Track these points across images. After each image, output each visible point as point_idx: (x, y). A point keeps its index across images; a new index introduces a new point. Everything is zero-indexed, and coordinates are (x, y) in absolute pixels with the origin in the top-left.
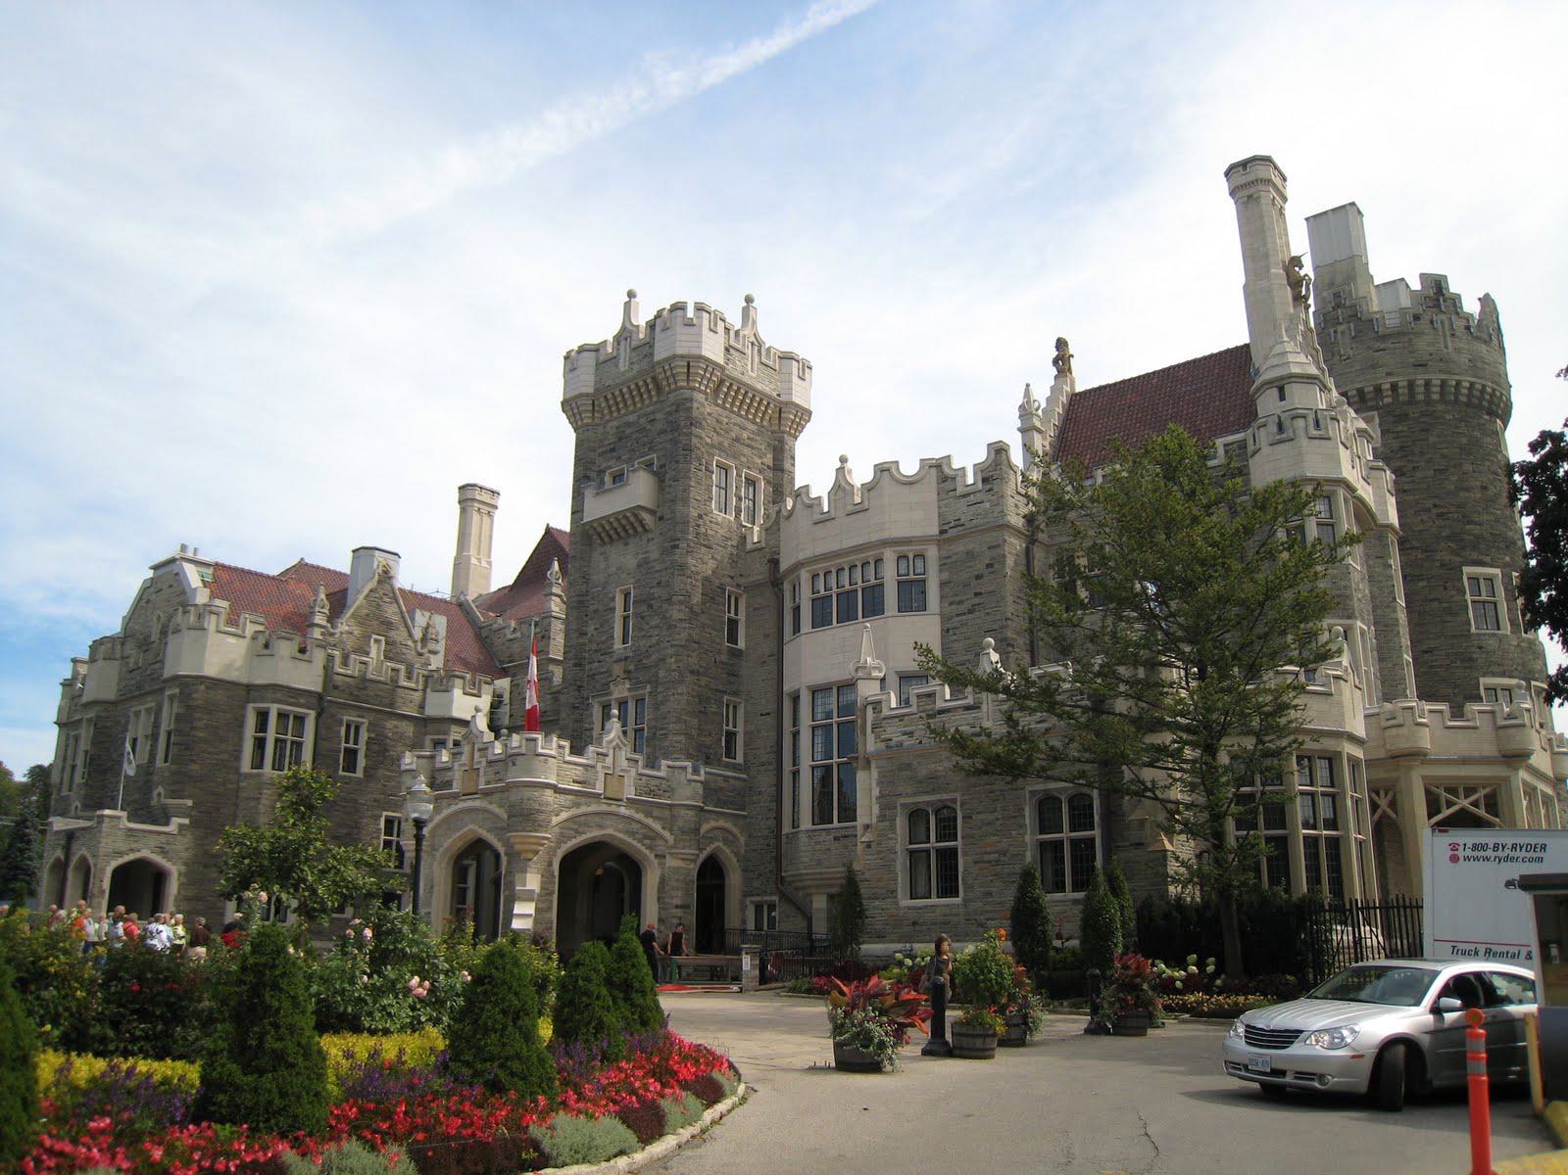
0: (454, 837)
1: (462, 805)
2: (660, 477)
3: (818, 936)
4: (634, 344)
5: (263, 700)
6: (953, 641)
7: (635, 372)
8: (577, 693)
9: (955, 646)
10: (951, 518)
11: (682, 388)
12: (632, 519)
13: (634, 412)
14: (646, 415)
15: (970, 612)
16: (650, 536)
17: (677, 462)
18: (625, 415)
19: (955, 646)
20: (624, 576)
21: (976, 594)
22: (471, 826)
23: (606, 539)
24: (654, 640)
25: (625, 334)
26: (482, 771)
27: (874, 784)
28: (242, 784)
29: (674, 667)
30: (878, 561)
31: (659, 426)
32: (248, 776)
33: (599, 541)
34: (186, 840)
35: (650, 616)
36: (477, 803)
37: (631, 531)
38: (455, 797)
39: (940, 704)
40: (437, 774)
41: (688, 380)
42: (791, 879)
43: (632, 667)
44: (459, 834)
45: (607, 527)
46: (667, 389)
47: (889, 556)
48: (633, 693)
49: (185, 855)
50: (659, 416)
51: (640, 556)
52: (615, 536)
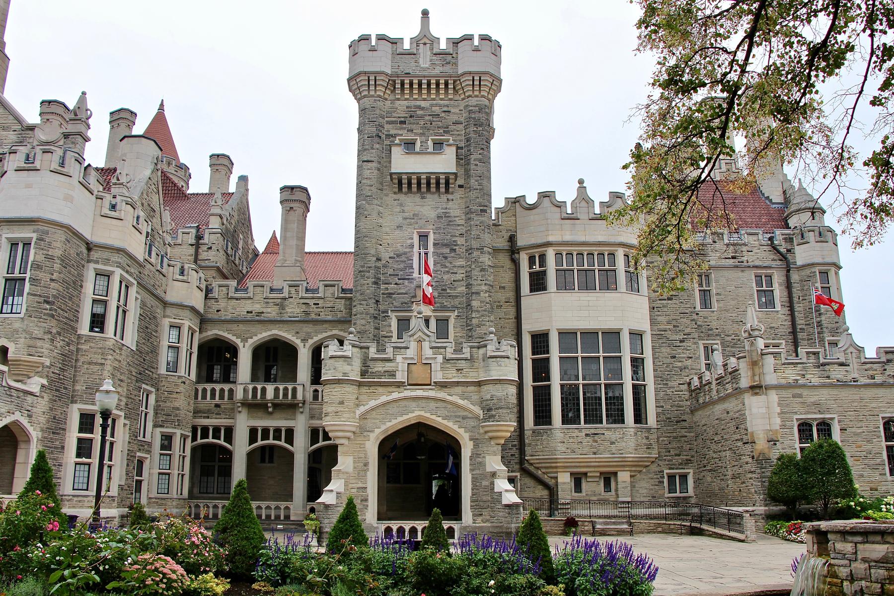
0: (394, 422)
2: (462, 159)
3: (563, 501)
5: (107, 261)
11: (483, 96)
12: (442, 181)
13: (424, 100)
14: (436, 105)
15: (669, 299)
16: (450, 197)
18: (416, 99)
20: (422, 222)
22: (417, 413)
23: (405, 189)
24: (459, 277)
25: (425, 39)
26: (436, 366)
27: (776, 405)
28: (84, 347)
29: (488, 300)
30: (612, 255)
31: (455, 118)
32: (89, 339)
33: (397, 190)
34: (44, 403)
35: (453, 257)
36: (431, 394)
37: (433, 190)
38: (399, 385)
39: (822, 360)
41: (488, 93)
42: (532, 462)
44: (400, 419)
45: (414, 181)
46: (471, 93)
47: (620, 253)
49: (42, 419)
50: (453, 110)
51: (440, 210)
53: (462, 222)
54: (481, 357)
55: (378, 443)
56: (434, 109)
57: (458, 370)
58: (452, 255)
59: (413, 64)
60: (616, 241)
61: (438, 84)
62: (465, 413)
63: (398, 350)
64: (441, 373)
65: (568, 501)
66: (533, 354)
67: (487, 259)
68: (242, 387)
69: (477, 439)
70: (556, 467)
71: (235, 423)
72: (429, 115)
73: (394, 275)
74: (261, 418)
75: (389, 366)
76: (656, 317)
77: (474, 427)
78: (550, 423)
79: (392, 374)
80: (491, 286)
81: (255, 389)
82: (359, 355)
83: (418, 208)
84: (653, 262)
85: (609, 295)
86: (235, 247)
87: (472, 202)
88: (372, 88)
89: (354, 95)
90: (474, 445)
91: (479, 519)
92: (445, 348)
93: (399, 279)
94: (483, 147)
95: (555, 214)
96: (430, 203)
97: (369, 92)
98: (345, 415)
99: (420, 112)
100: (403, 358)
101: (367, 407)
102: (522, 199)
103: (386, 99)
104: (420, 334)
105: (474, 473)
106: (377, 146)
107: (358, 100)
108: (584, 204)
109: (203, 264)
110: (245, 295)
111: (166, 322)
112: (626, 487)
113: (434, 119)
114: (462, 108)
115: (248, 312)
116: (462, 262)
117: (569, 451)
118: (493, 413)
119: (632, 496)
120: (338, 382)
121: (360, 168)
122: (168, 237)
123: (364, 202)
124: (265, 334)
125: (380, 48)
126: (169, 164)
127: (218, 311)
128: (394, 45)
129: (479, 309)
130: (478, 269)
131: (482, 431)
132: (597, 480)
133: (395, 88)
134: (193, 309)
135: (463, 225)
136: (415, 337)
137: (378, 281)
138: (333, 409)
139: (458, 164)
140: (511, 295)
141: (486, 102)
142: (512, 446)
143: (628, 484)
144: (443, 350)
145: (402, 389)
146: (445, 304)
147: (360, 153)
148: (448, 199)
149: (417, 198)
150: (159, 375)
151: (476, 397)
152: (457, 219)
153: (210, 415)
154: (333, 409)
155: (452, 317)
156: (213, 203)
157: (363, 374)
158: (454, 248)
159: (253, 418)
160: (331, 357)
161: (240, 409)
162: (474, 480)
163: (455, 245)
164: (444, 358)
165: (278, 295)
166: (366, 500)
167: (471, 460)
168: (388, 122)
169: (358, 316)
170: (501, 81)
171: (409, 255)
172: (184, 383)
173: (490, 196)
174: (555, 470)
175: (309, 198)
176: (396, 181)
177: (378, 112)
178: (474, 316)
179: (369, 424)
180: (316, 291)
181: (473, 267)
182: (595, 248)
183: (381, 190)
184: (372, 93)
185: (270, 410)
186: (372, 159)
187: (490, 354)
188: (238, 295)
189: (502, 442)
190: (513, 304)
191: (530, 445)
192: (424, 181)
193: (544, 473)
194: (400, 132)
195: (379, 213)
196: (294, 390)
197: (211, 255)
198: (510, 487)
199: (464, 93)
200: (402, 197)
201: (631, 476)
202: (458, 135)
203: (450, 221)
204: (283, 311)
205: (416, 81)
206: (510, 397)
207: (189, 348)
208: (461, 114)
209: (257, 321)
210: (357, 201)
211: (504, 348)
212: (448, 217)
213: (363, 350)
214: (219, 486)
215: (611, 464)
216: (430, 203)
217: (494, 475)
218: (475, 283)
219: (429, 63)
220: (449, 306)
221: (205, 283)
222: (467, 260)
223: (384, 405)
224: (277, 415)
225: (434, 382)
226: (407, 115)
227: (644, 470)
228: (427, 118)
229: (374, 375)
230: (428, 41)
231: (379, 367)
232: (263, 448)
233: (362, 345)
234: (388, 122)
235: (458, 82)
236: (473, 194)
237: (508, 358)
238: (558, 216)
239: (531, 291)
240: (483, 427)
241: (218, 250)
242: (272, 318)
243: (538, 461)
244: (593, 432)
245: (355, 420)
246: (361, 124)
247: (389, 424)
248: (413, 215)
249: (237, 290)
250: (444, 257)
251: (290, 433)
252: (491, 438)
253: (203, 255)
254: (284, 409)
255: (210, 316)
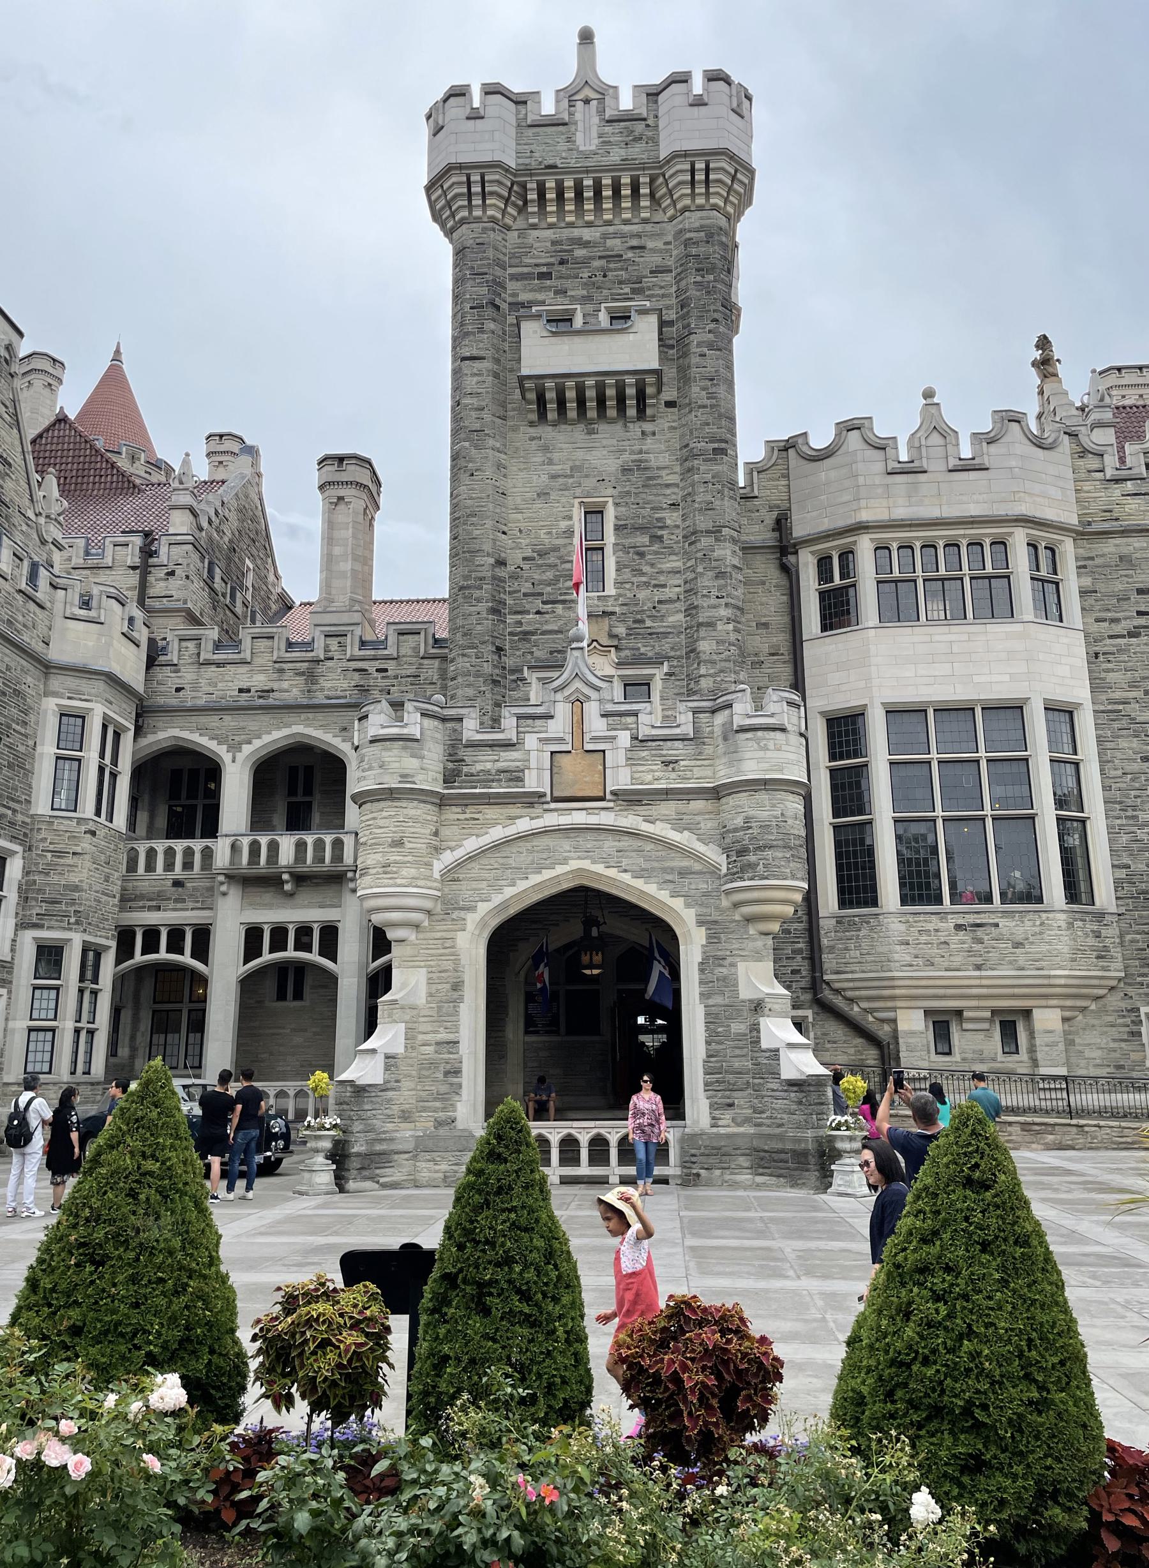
0: (522, 885)
1: (551, 820)
3: (913, 1073)
4: (608, 114)
6: (1108, 671)
7: (616, 155)
8: (496, 657)
9: (1111, 677)
10: (1094, 508)
11: (715, 208)
13: (589, 225)
14: (615, 235)
15: (1131, 635)
16: (648, 427)
17: (715, 320)
18: (571, 225)
19: (1111, 677)
20: (590, 483)
21: (1140, 613)
22: (574, 864)
23: (552, 415)
24: (670, 593)
26: (616, 757)
29: (733, 637)
30: (1000, 543)
31: (656, 260)
33: (534, 417)
35: (656, 553)
36: (607, 819)
37: (612, 413)
38: (533, 800)
40: (462, 753)
41: (726, 200)
42: (837, 985)
43: (621, 630)
44: (535, 879)
46: (687, 201)
47: (1019, 539)
48: (620, 672)
50: (650, 244)
51: (626, 457)
52: (572, 414)
53: (674, 479)
54: (718, 731)
55: (486, 934)
56: (609, 243)
57: (666, 764)
58: (655, 547)
59: (562, 146)
60: (1010, 513)
61: (616, 188)
62: (686, 863)
63: (530, 722)
64: (628, 770)
65: (924, 1073)
66: (833, 757)
67: (728, 552)
68: (228, 841)
69: (716, 922)
70: (893, 998)
71: (215, 917)
72: (600, 258)
73: (533, 595)
74: (269, 906)
75: (508, 759)
76: (1103, 675)
77: (706, 894)
78: (874, 902)
79: (516, 776)
80: (738, 608)
81: (255, 848)
82: (439, 736)
83: (580, 455)
84: (1092, 558)
85: (998, 630)
86: (237, 586)
87: (695, 434)
88: (477, 201)
89: (443, 226)
90: (709, 937)
91: (727, 1117)
92: (635, 714)
93: (544, 603)
94: (716, 315)
95: (875, 464)
96: (605, 442)
97: (470, 212)
98: (404, 872)
99: (580, 253)
100: (540, 740)
101: (460, 853)
102: (800, 441)
103: (509, 228)
104: (578, 684)
105: (711, 1002)
106: (491, 325)
107: (449, 233)
108: (936, 439)
109: (157, 604)
110: (235, 656)
111: (51, 705)
112: (1054, 1044)
113: (612, 266)
114: (670, 238)
115: (241, 691)
116: (674, 563)
117: (920, 961)
118: (752, 858)
119: (1068, 1064)
120: (391, 795)
121: (456, 373)
122: (52, 528)
123: (467, 444)
124: (277, 735)
125: (490, 112)
126: (133, 459)
127: (178, 690)
128: (519, 107)
129: (715, 657)
130: (710, 574)
131: (725, 903)
132: (986, 1026)
133: (526, 202)
134: (112, 680)
135: (677, 485)
136: (567, 692)
137: (500, 607)
138: (378, 857)
139: (663, 357)
140: (781, 639)
141: (723, 222)
142: (793, 952)
143: (1058, 1037)
144: (630, 720)
145: (538, 810)
146: (643, 650)
147: (456, 341)
148: (643, 433)
149: (578, 433)
150: (32, 816)
151: (710, 824)
152: (663, 473)
153: (163, 904)
154: (378, 857)
155: (658, 677)
156: (176, 484)
157: (449, 778)
158: (660, 533)
159: (254, 905)
160: (374, 741)
161: (224, 888)
162: (712, 1020)
163: (661, 528)
164: (635, 738)
165: (303, 654)
166: (457, 1072)
167: (702, 971)
168: (514, 277)
169: (460, 679)
170: (751, 172)
171: (563, 551)
172: (93, 833)
173: (732, 419)
174: (889, 1004)
175: (378, 484)
176: (532, 396)
177: (490, 253)
178: (703, 671)
179: (465, 890)
180: (382, 644)
181: (700, 569)
182: (962, 532)
183: (504, 418)
184: (477, 213)
185: (288, 887)
186: (481, 353)
187: (738, 721)
188: (220, 657)
189: (775, 927)
190: (787, 657)
191: (832, 949)
192: (591, 394)
193: (865, 1010)
194: (540, 297)
195: (499, 466)
196: (338, 844)
197: (174, 587)
198: (797, 1038)
199: (674, 203)
200: (546, 431)
201: (1065, 1020)
202: (663, 296)
203: (650, 478)
204: (314, 687)
205: (569, 183)
206: (790, 822)
207: (108, 760)
208: (667, 251)
209: (261, 708)
210: (453, 444)
211: (772, 708)
212: (646, 469)
213: (449, 725)
214: (190, 1052)
215: (1017, 991)
216: (605, 442)
217: (758, 1007)
218: (705, 603)
219: (596, 141)
220: (650, 654)
221: (145, 630)
222: (687, 556)
223: (497, 846)
224: (305, 896)
225: (613, 793)
226: (552, 260)
227: (1093, 1007)
228: (597, 263)
229: (474, 779)
230: (593, 95)
231: (485, 762)
232: (282, 968)
233: (447, 712)
234: (514, 277)
235: (661, 180)
236: (696, 418)
237: (783, 730)
238: (879, 467)
239: (824, 628)
240: (728, 893)
241: (187, 577)
242: (291, 702)
243: (851, 985)
244: (971, 921)
245: (429, 884)
246: (458, 281)
247: (509, 892)
248: (572, 469)
249: (218, 646)
250: (638, 553)
251: (330, 933)
252: (750, 919)
253: (158, 587)
254: (317, 884)
255: (161, 701)
